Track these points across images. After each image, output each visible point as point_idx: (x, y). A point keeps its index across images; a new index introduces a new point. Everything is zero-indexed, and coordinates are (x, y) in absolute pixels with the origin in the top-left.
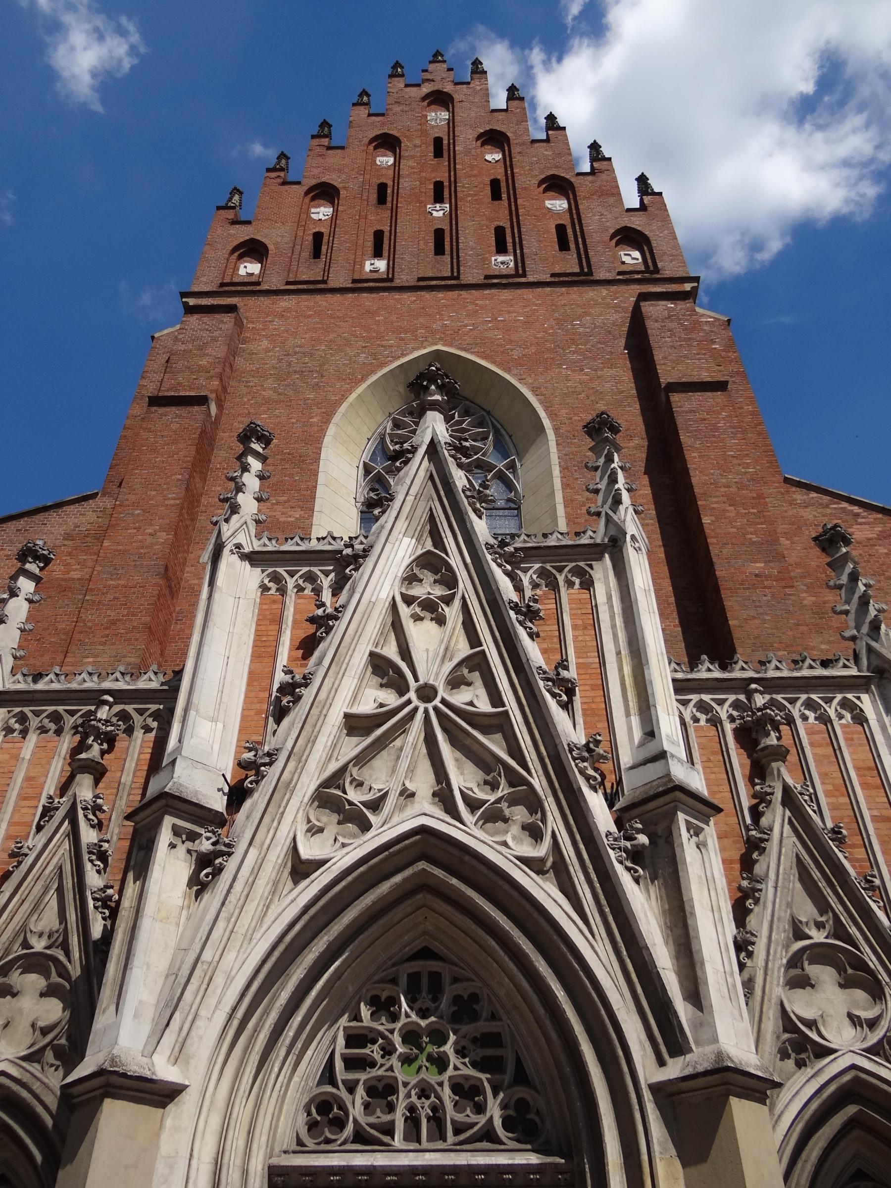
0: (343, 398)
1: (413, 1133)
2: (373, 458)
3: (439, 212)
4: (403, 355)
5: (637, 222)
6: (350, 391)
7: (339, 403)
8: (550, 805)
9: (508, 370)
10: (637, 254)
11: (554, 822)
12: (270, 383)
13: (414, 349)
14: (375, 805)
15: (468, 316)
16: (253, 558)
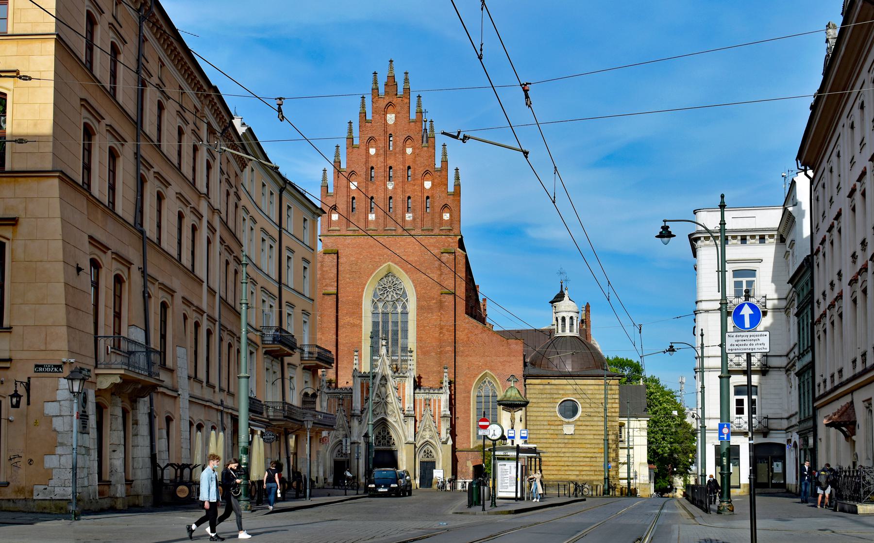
0: (366, 282)
1: (383, 445)
2: (374, 296)
3: (390, 186)
4: (381, 266)
5: (449, 201)
6: (368, 280)
7: (365, 284)
8: (397, 415)
9: (407, 273)
10: (448, 215)
11: (397, 417)
12: (348, 276)
13: (384, 263)
14: (378, 414)
15: (398, 249)
16: (359, 377)
